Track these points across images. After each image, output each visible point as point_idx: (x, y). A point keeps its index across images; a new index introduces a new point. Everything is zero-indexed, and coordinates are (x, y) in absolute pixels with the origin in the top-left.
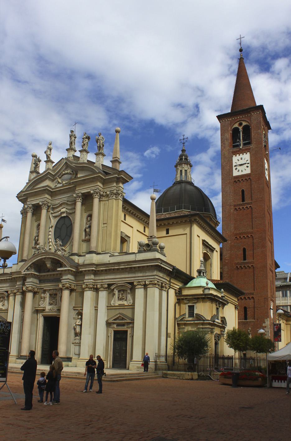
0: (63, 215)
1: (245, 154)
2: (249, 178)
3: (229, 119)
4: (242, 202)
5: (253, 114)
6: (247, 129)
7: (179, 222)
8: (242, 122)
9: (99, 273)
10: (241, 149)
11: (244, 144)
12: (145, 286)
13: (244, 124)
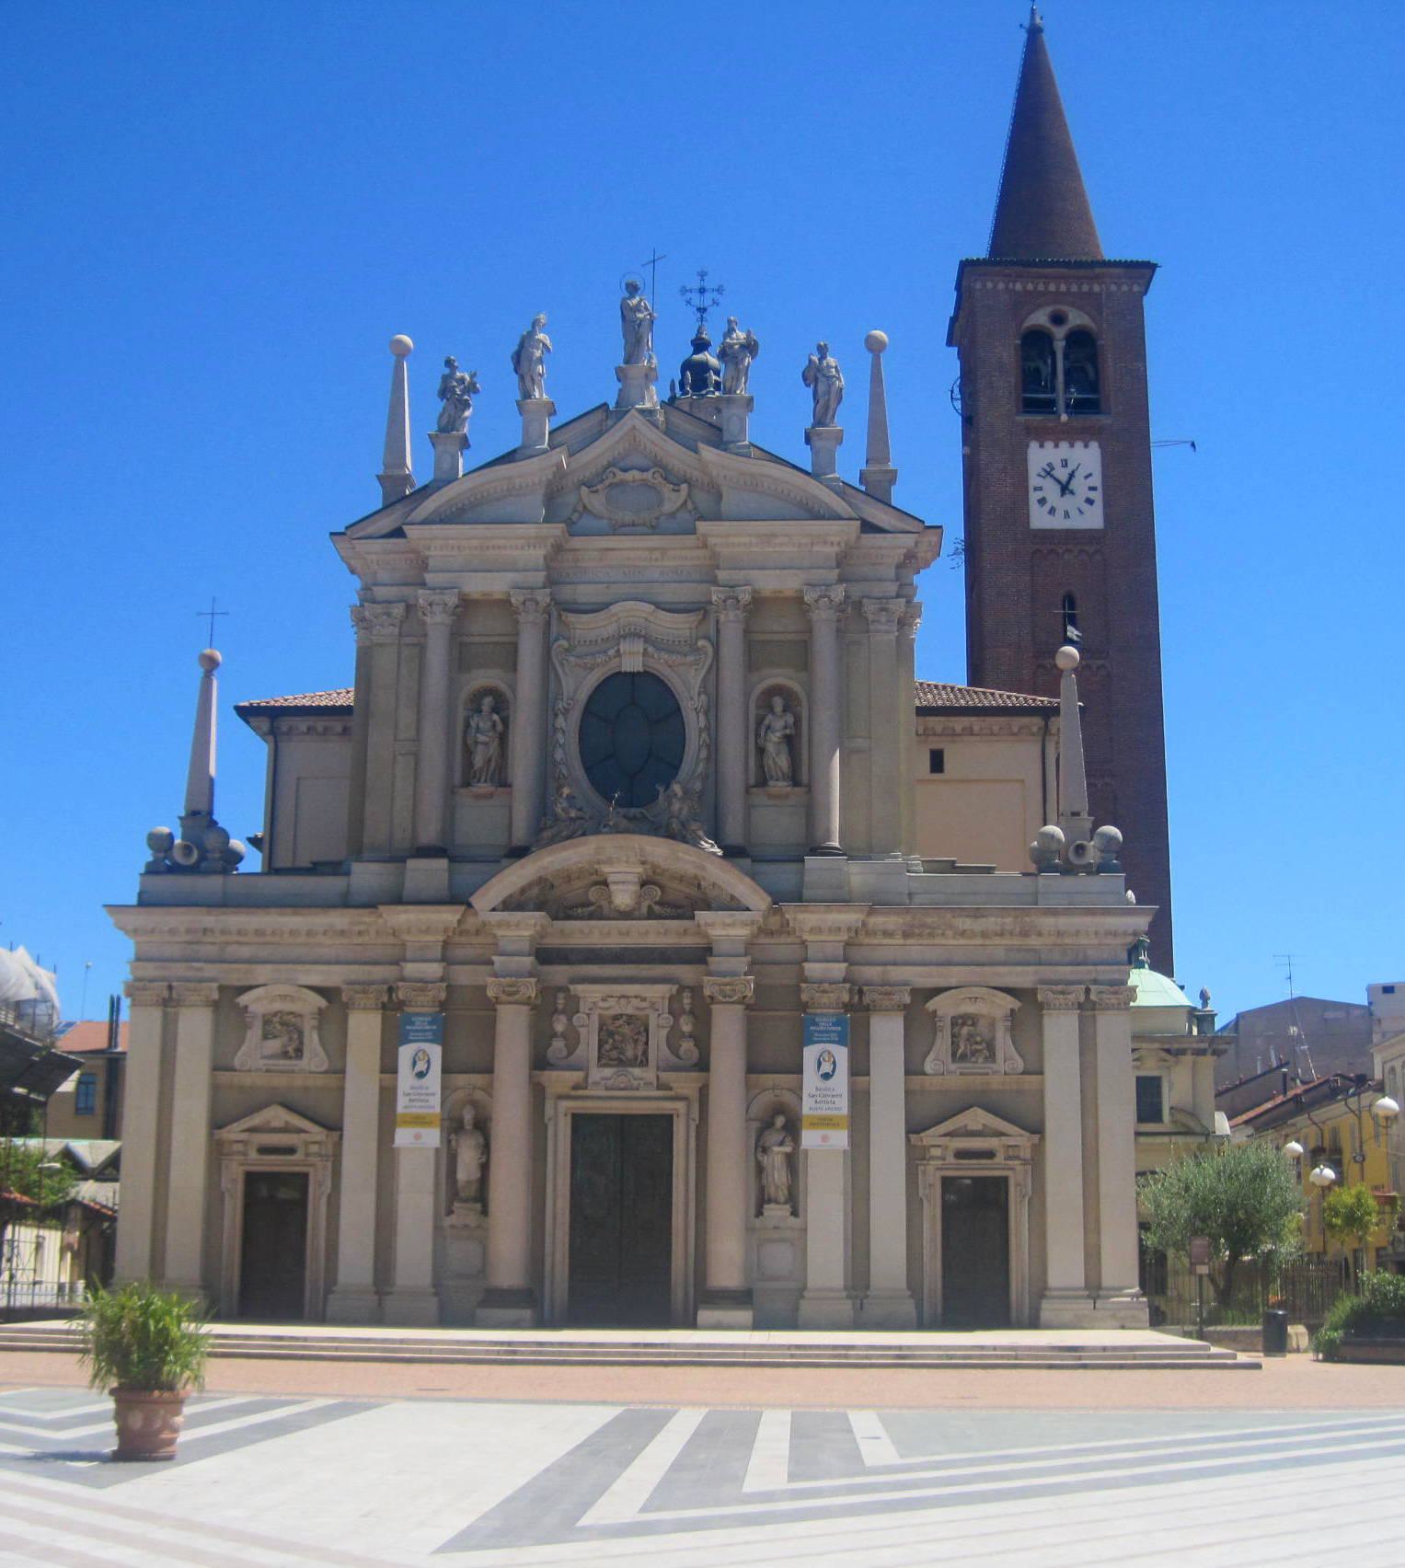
0: (632, 664)
1: (1079, 445)
2: (1096, 552)
5: (1113, 288)
8: (1064, 308)
10: (1065, 424)
12: (1087, 1009)
13: (1076, 318)
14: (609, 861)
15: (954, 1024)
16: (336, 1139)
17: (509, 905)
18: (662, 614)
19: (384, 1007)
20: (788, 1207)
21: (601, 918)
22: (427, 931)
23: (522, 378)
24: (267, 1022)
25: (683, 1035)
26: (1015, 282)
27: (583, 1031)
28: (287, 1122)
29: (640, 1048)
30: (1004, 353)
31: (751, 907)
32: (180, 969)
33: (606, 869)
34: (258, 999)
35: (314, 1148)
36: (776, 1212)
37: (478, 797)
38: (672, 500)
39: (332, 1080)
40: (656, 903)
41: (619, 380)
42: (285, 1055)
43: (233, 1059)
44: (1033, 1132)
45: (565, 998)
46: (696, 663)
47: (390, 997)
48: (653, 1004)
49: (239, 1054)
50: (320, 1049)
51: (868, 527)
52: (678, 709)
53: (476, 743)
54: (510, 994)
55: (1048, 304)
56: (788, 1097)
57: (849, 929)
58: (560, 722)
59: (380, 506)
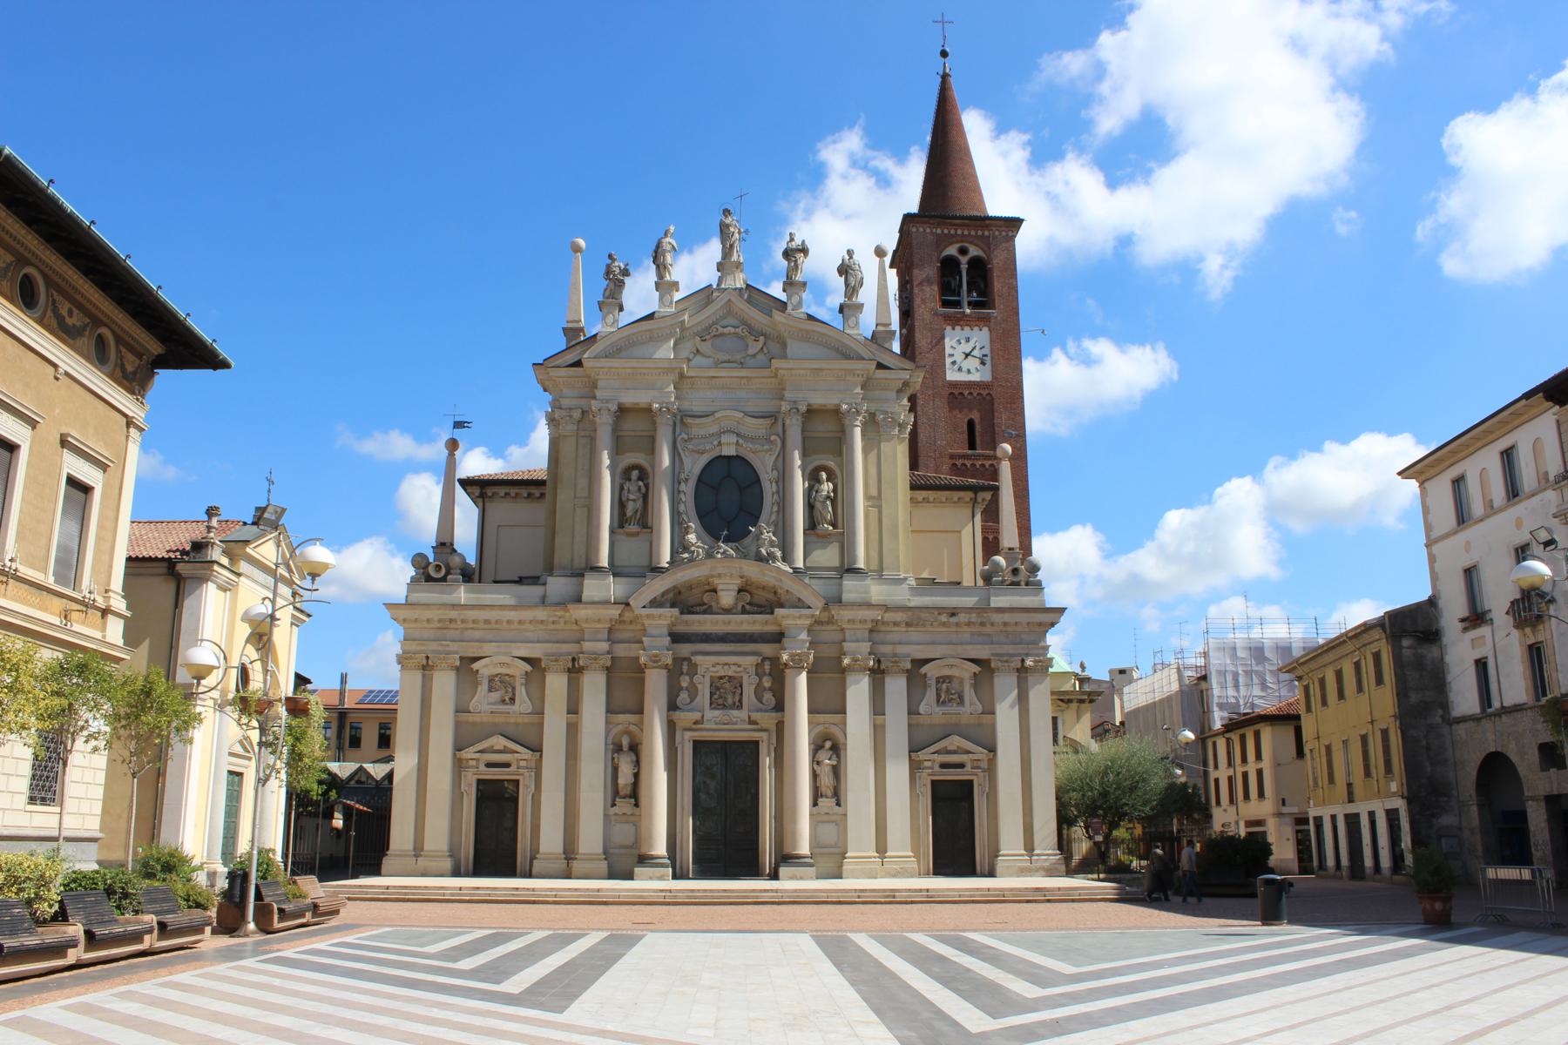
0: (729, 451)
1: (976, 329)
2: (989, 394)
3: (934, 230)
4: (969, 449)
5: (997, 233)
6: (980, 270)
7: (944, 500)
9: (883, 628)
11: (971, 304)
13: (974, 251)
14: (719, 575)
15: (938, 682)
16: (538, 757)
17: (654, 603)
18: (748, 419)
19: (569, 671)
20: (834, 800)
21: (712, 613)
22: (599, 621)
23: (658, 267)
24: (491, 680)
25: (765, 689)
26: (936, 228)
27: (700, 686)
28: (505, 746)
29: (737, 698)
30: (927, 272)
31: (811, 606)
32: (433, 646)
33: (716, 581)
34: (486, 666)
35: (523, 763)
36: (826, 803)
37: (630, 535)
38: (754, 348)
39: (535, 719)
40: (749, 604)
41: (718, 270)
42: (503, 701)
43: (469, 704)
44: (990, 751)
45: (688, 665)
46: (770, 450)
47: (573, 665)
48: (745, 669)
49: (473, 701)
50: (526, 699)
51: (880, 366)
52: (758, 480)
53: (628, 499)
54: (655, 662)
55: (957, 242)
56: (835, 730)
57: (872, 621)
58: (683, 487)
59: (564, 347)
